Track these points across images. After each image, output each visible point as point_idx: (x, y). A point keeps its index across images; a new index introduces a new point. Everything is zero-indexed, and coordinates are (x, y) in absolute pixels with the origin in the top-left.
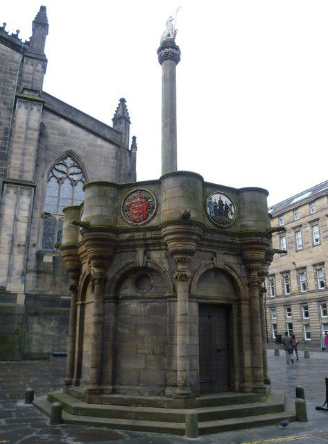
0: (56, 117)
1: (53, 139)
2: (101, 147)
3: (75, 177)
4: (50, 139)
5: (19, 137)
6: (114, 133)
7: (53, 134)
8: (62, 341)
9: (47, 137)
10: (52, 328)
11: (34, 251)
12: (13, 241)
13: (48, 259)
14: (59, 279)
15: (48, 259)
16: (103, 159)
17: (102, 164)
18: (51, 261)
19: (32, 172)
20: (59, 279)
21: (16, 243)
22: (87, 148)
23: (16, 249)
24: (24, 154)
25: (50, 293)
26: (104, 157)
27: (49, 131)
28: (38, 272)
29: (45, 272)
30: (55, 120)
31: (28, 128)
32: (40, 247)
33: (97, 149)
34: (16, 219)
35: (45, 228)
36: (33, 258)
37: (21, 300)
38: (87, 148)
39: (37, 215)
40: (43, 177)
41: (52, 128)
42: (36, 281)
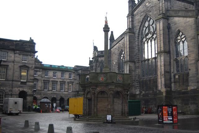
0: (173, 18)
1: (173, 27)
2: (189, 21)
3: (183, 40)
4: (172, 29)
5: (158, 36)
6: (193, 12)
7: (173, 26)
8: (183, 108)
9: (171, 28)
10: (180, 103)
11: (172, 75)
12: (161, 74)
13: (177, 77)
14: (181, 83)
15: (177, 77)
16: (190, 27)
17: (190, 29)
18: (178, 77)
19: (163, 47)
20: (181, 83)
21: (162, 74)
22: (184, 25)
23: (162, 76)
24: (160, 41)
25: (179, 89)
26: (191, 26)
27: (171, 25)
28: (175, 82)
29: (177, 82)
30: (172, 19)
31: (160, 31)
32: (176, 72)
33: (187, 24)
34: (161, 66)
35: (177, 65)
36: (172, 77)
37: (164, 94)
38: (184, 25)
39: (172, 60)
40: (172, 45)
41: (172, 23)
42: (175, 86)
